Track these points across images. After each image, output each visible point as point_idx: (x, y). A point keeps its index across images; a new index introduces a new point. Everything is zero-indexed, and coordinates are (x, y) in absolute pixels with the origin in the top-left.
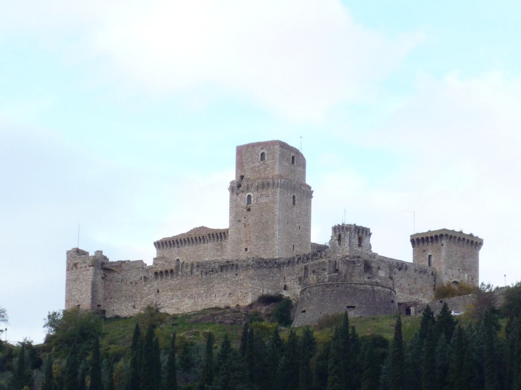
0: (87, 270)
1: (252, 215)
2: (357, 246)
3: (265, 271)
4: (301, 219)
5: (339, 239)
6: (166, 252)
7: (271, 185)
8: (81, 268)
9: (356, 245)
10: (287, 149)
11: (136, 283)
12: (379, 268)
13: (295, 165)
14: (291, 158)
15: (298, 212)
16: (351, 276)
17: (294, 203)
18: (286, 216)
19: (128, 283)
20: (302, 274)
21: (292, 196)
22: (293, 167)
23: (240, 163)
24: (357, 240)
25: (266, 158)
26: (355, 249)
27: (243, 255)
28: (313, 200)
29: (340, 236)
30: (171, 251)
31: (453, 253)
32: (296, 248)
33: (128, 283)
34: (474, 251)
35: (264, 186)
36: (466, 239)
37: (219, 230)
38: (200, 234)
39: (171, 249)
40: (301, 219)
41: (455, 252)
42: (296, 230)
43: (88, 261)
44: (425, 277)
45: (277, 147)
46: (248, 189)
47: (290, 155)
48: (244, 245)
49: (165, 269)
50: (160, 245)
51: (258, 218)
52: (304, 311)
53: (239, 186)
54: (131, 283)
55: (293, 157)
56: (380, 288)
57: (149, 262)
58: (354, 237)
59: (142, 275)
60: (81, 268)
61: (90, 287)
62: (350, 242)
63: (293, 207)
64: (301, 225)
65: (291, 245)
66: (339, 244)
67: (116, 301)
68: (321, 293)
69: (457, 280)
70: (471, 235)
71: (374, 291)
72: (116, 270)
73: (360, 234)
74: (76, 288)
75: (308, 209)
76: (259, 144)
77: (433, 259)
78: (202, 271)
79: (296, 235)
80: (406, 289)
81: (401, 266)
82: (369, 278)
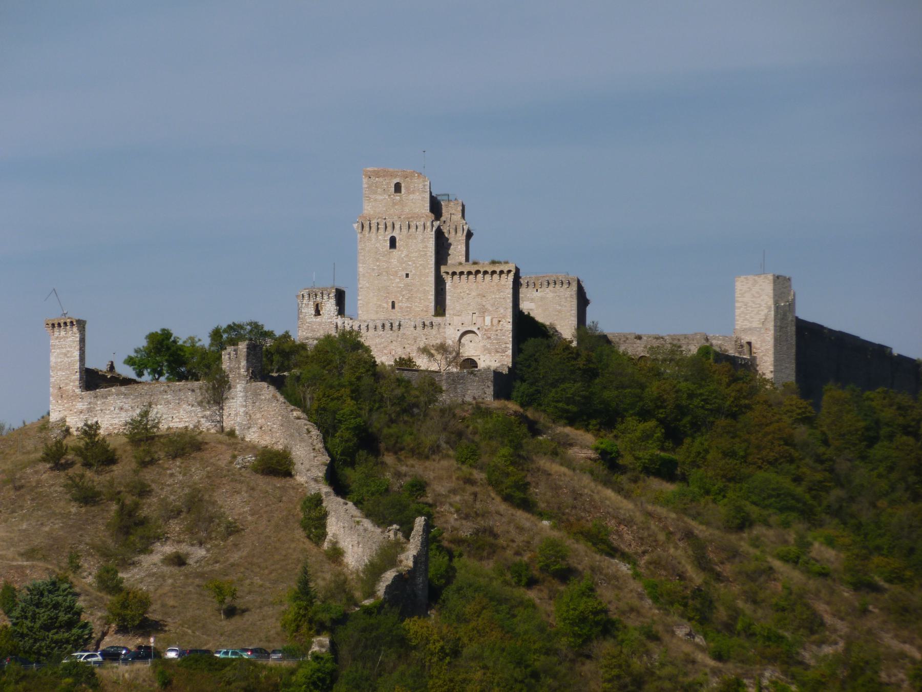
4: (410, 263)
10: (384, 176)
21: (389, 237)
24: (313, 309)
32: (400, 304)
36: (482, 270)
40: (410, 263)
41: (467, 292)
47: (388, 184)
58: (307, 305)
63: (390, 252)
64: (411, 271)
65: (387, 303)
69: (469, 329)
73: (319, 299)
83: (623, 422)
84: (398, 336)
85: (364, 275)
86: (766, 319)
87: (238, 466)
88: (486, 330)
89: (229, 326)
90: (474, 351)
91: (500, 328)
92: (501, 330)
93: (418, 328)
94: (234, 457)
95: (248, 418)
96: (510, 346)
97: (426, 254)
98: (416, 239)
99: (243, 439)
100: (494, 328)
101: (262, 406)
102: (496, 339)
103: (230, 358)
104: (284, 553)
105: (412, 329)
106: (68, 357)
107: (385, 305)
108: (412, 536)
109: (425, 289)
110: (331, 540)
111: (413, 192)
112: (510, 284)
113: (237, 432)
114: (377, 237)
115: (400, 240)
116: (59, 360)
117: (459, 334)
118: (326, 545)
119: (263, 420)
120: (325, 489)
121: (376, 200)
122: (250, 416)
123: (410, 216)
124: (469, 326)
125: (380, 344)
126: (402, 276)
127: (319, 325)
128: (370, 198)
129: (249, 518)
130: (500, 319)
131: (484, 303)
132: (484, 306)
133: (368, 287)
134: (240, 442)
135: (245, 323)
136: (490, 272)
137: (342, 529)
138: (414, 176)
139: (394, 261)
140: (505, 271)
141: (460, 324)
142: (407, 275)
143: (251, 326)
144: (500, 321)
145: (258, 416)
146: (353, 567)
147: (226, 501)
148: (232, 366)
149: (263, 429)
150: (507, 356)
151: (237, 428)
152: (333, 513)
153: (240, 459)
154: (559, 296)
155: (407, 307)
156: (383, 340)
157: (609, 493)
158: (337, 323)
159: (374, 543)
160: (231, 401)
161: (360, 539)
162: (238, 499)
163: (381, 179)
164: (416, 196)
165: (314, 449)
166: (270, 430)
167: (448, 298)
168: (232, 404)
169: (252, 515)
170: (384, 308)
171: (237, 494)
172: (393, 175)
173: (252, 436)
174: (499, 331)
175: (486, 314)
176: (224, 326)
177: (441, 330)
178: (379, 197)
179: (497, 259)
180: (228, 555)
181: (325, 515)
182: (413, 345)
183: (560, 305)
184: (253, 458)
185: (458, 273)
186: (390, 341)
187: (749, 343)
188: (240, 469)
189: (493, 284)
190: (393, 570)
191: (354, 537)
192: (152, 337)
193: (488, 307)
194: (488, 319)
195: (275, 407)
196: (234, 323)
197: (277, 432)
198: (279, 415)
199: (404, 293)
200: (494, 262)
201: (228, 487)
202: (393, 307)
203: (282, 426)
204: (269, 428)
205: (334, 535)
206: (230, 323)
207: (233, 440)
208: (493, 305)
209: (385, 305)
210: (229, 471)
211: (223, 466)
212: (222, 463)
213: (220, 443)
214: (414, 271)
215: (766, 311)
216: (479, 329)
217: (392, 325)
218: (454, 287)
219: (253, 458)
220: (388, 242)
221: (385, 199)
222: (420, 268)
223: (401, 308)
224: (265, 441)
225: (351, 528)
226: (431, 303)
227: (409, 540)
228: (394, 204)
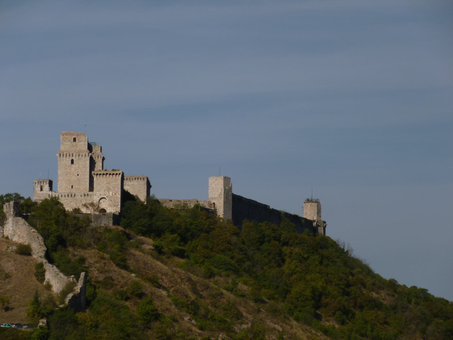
2: (39, 191)
4: (79, 170)
9: (39, 190)
10: (69, 135)
13: (77, 142)
14: (73, 139)
15: (76, 167)
18: (65, 172)
21: (70, 160)
22: (75, 144)
24: (39, 188)
26: (38, 193)
31: (100, 183)
32: (75, 186)
36: (109, 173)
40: (79, 170)
41: (103, 182)
42: (74, 177)
58: (37, 186)
63: (71, 166)
64: (80, 173)
65: (70, 186)
73: (42, 184)
79: (75, 180)
83: (164, 235)
84: (74, 199)
85: (60, 174)
86: (220, 194)
87: (10, 251)
88: (110, 197)
89: (6, 195)
90: (105, 206)
91: (116, 196)
92: (116, 197)
93: (82, 196)
94: (8, 247)
95: (14, 232)
96: (120, 204)
97: (86, 167)
98: (82, 160)
99: (12, 240)
100: (113, 197)
101: (20, 227)
102: (114, 201)
103: (7, 207)
104: (28, 286)
105: (80, 196)
107: (69, 187)
108: (79, 280)
109: (85, 180)
110: (47, 281)
111: (81, 142)
112: (120, 179)
113: (9, 237)
114: (66, 159)
115: (75, 161)
117: (99, 199)
118: (45, 283)
119: (20, 233)
120: (44, 261)
121: (65, 145)
122: (15, 231)
123: (79, 151)
124: (103, 195)
125: (67, 203)
126: (76, 175)
127: (42, 195)
128: (63, 144)
129: (14, 272)
130: (116, 193)
131: (109, 186)
132: (109, 188)
133: (62, 180)
134: (11, 241)
135: (13, 193)
136: (112, 174)
137: (51, 277)
138: (81, 135)
139: (73, 169)
140: (118, 174)
141: (99, 195)
142: (78, 175)
143: (15, 195)
144: (115, 194)
145: (18, 231)
146: (56, 292)
147: (5, 265)
148: (7, 211)
149: (20, 236)
150: (118, 208)
151: (9, 235)
152: (48, 270)
153: (10, 248)
154: (139, 184)
155: (78, 188)
156: (68, 201)
157: (158, 263)
158: (49, 194)
159: (64, 282)
160: (7, 225)
161: (58, 281)
162: (10, 264)
163: (68, 136)
164: (82, 143)
165: (40, 245)
166: (23, 237)
167: (95, 184)
168: (7, 226)
169: (15, 270)
170: (68, 188)
171: (10, 262)
172: (72, 135)
173: (15, 239)
174: (115, 198)
175: (110, 191)
176: (4, 194)
177: (92, 197)
178: (68, 143)
179: (115, 169)
180: (6, 286)
181: (44, 271)
182: (80, 203)
183: (140, 188)
184: (16, 248)
185: (99, 174)
186: (70, 201)
187: (214, 203)
188: (11, 252)
189: (113, 179)
190: (72, 293)
191: (56, 280)
193: (111, 188)
194: (111, 193)
195: (24, 227)
196: (8, 194)
197: (25, 238)
198: (26, 231)
199: (76, 182)
200: (113, 170)
201: (6, 259)
202: (72, 187)
203: (27, 235)
204: (22, 236)
205: (48, 279)
206: (7, 193)
207: (7, 241)
208: (113, 187)
209: (69, 187)
210: (6, 253)
211: (4, 251)
212: (4, 250)
213: (3, 241)
214: (81, 173)
215: (221, 191)
216: (107, 197)
217: (71, 195)
218: (97, 180)
219: (16, 248)
220: (71, 161)
221: (69, 144)
222: (83, 172)
223: (75, 188)
224: (21, 241)
225: (55, 276)
226: (87, 186)
227: (78, 281)
228: (73, 146)
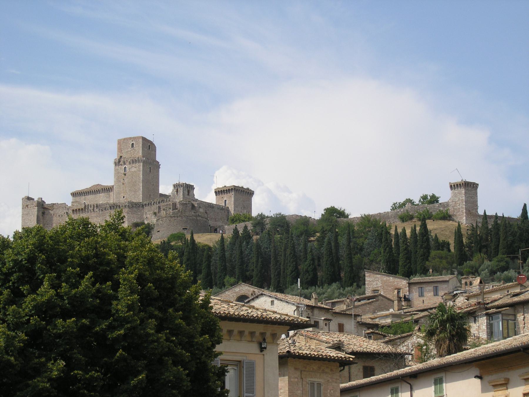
0: (34, 209)
1: (127, 178)
3: (135, 209)
5: (177, 191)
6: (78, 199)
7: (137, 161)
8: (30, 207)
11: (62, 216)
12: (200, 207)
16: (185, 211)
17: (150, 172)
19: (57, 216)
20: (156, 211)
21: (149, 167)
23: (120, 149)
25: (134, 146)
27: (122, 200)
28: (160, 169)
29: (177, 189)
30: (80, 198)
33: (57, 216)
34: (249, 198)
35: (134, 161)
37: (108, 186)
38: (97, 189)
39: (81, 197)
42: (151, 186)
43: (34, 204)
44: (223, 212)
45: (141, 140)
46: (125, 163)
47: (147, 144)
48: (122, 195)
49: (78, 208)
50: (74, 194)
51: (130, 180)
52: (159, 231)
53: (119, 162)
54: (59, 216)
55: (149, 146)
56: (200, 218)
57: (69, 205)
58: (185, 190)
59: (65, 211)
60: (30, 207)
61: (36, 218)
62: (183, 193)
66: (177, 194)
67: (50, 226)
68: (168, 221)
70: (248, 189)
71: (197, 220)
72: (50, 208)
74: (28, 219)
75: (157, 175)
76: (130, 138)
77: (227, 202)
78: (99, 209)
80: (213, 219)
81: (210, 206)
82: (195, 213)
106: (473, 199)
116: (469, 199)
163: (146, 142)
192: (253, 192)
